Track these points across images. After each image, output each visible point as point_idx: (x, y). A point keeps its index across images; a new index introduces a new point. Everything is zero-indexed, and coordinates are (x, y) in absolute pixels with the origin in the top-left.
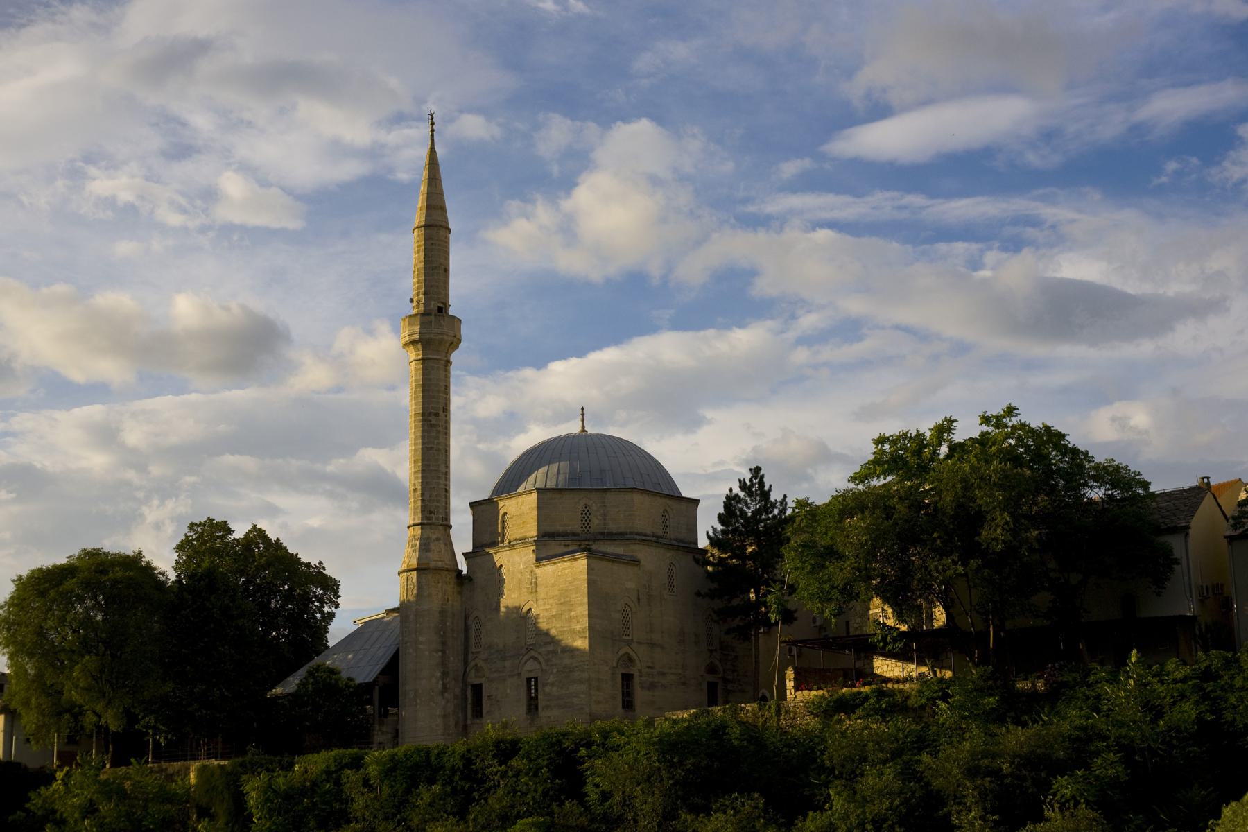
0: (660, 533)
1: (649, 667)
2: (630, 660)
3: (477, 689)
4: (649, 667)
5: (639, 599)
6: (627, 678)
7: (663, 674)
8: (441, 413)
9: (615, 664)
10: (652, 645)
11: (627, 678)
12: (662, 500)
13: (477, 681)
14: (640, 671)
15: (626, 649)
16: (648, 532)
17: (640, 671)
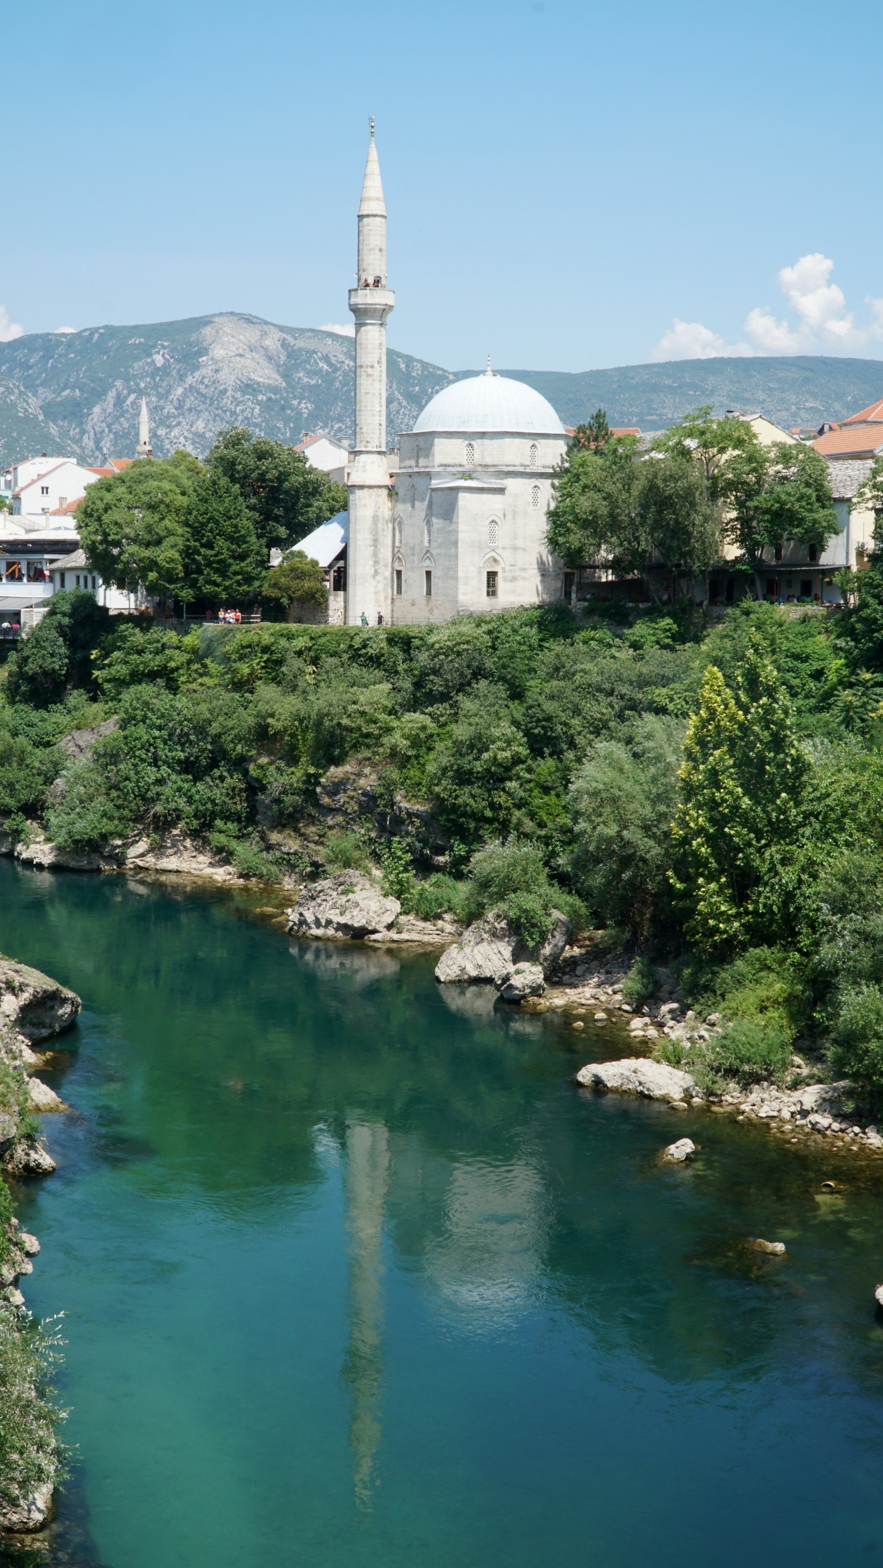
0: (528, 462)
1: (512, 565)
2: (495, 561)
3: (399, 573)
4: (512, 565)
5: (505, 516)
6: (492, 576)
7: (525, 569)
8: (376, 365)
9: (481, 565)
10: (515, 548)
11: (492, 576)
12: (532, 437)
13: (399, 568)
14: (503, 569)
15: (493, 554)
16: (517, 463)
17: (503, 569)
